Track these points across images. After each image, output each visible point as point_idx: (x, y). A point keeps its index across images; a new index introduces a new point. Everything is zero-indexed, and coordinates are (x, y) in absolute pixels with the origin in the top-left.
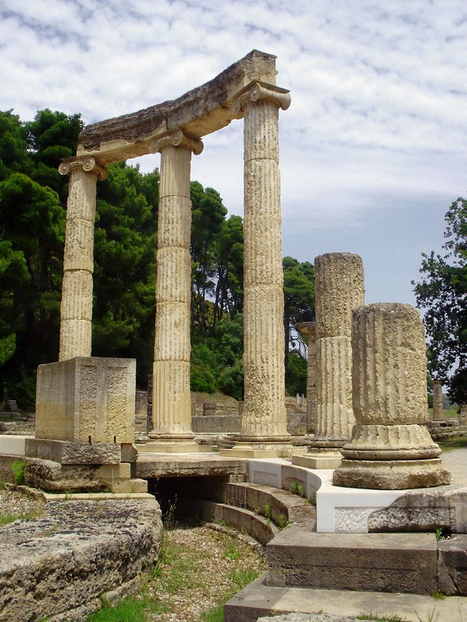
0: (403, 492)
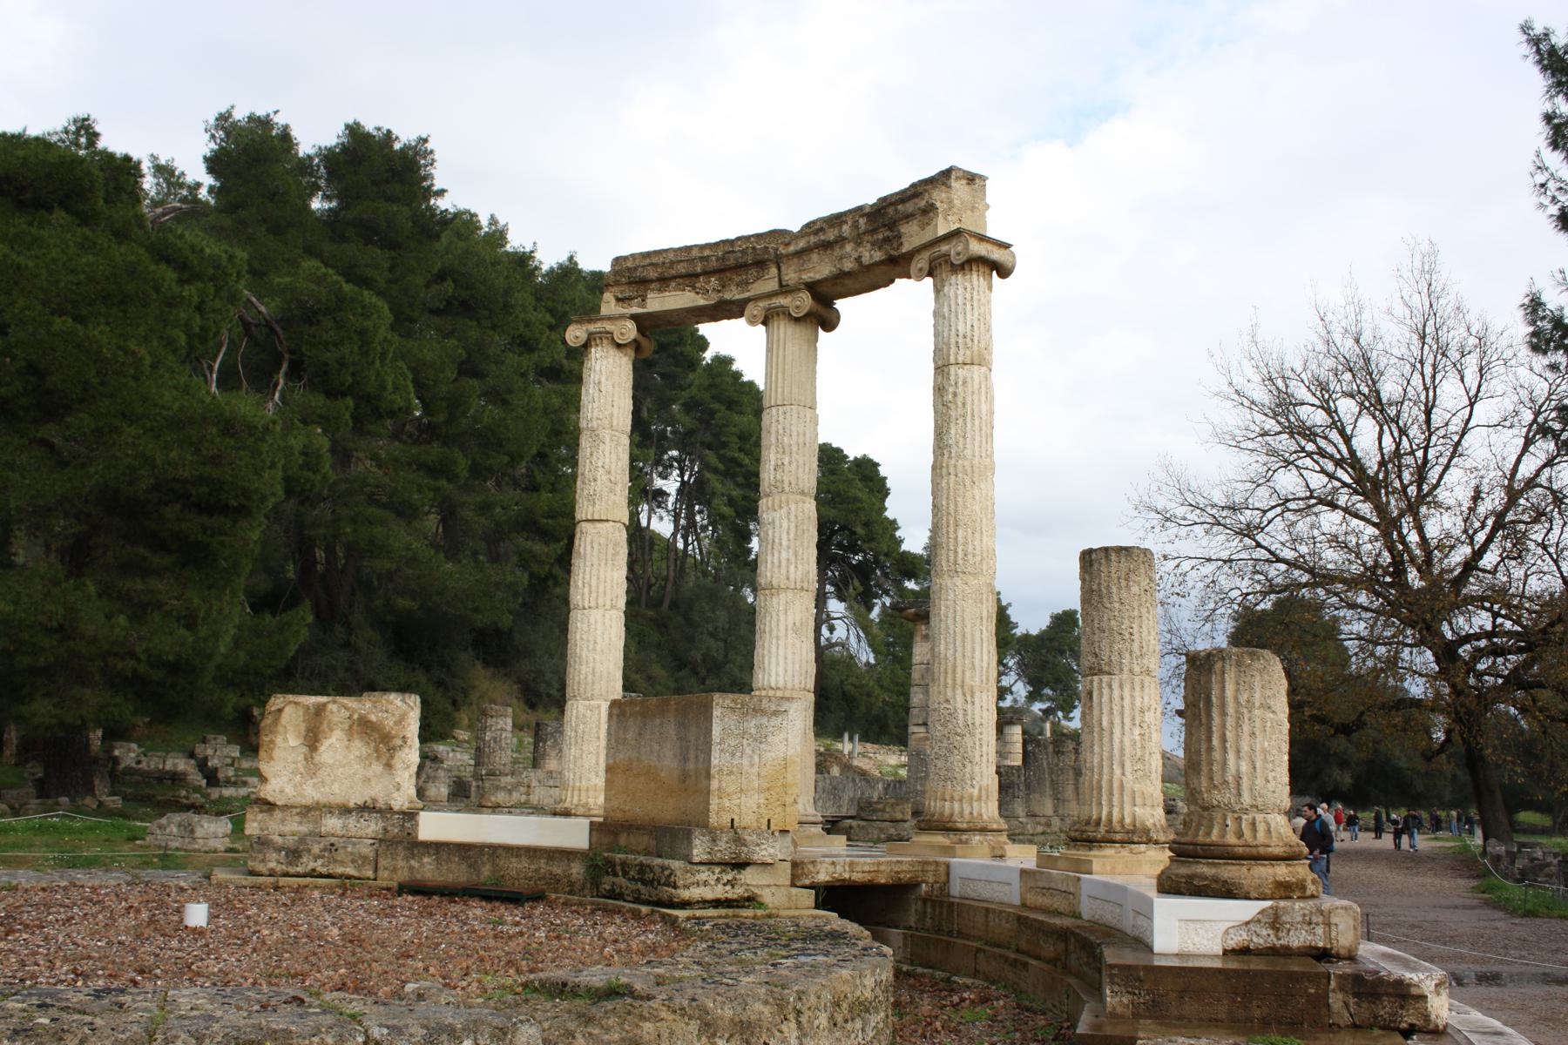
0: (1268, 903)
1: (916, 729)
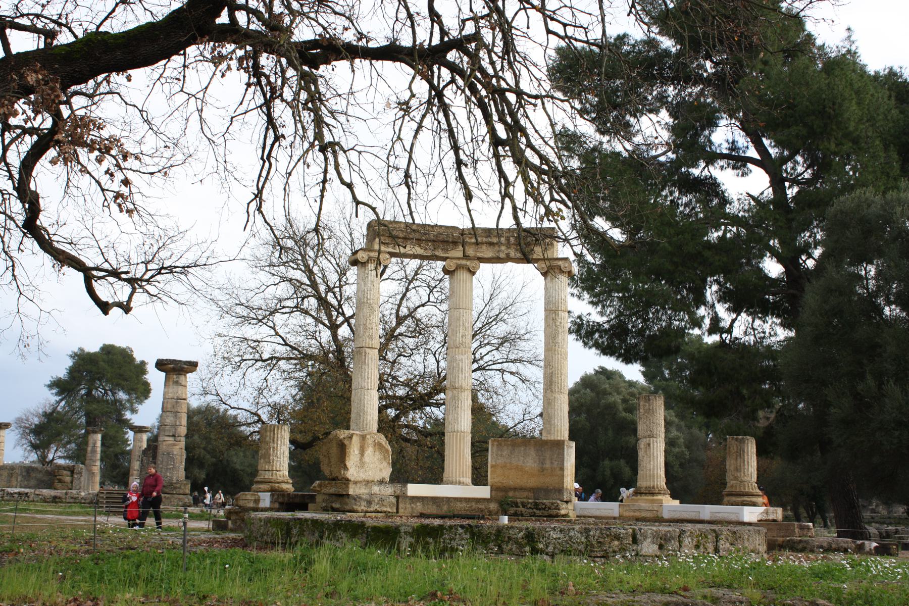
1: (167, 438)
